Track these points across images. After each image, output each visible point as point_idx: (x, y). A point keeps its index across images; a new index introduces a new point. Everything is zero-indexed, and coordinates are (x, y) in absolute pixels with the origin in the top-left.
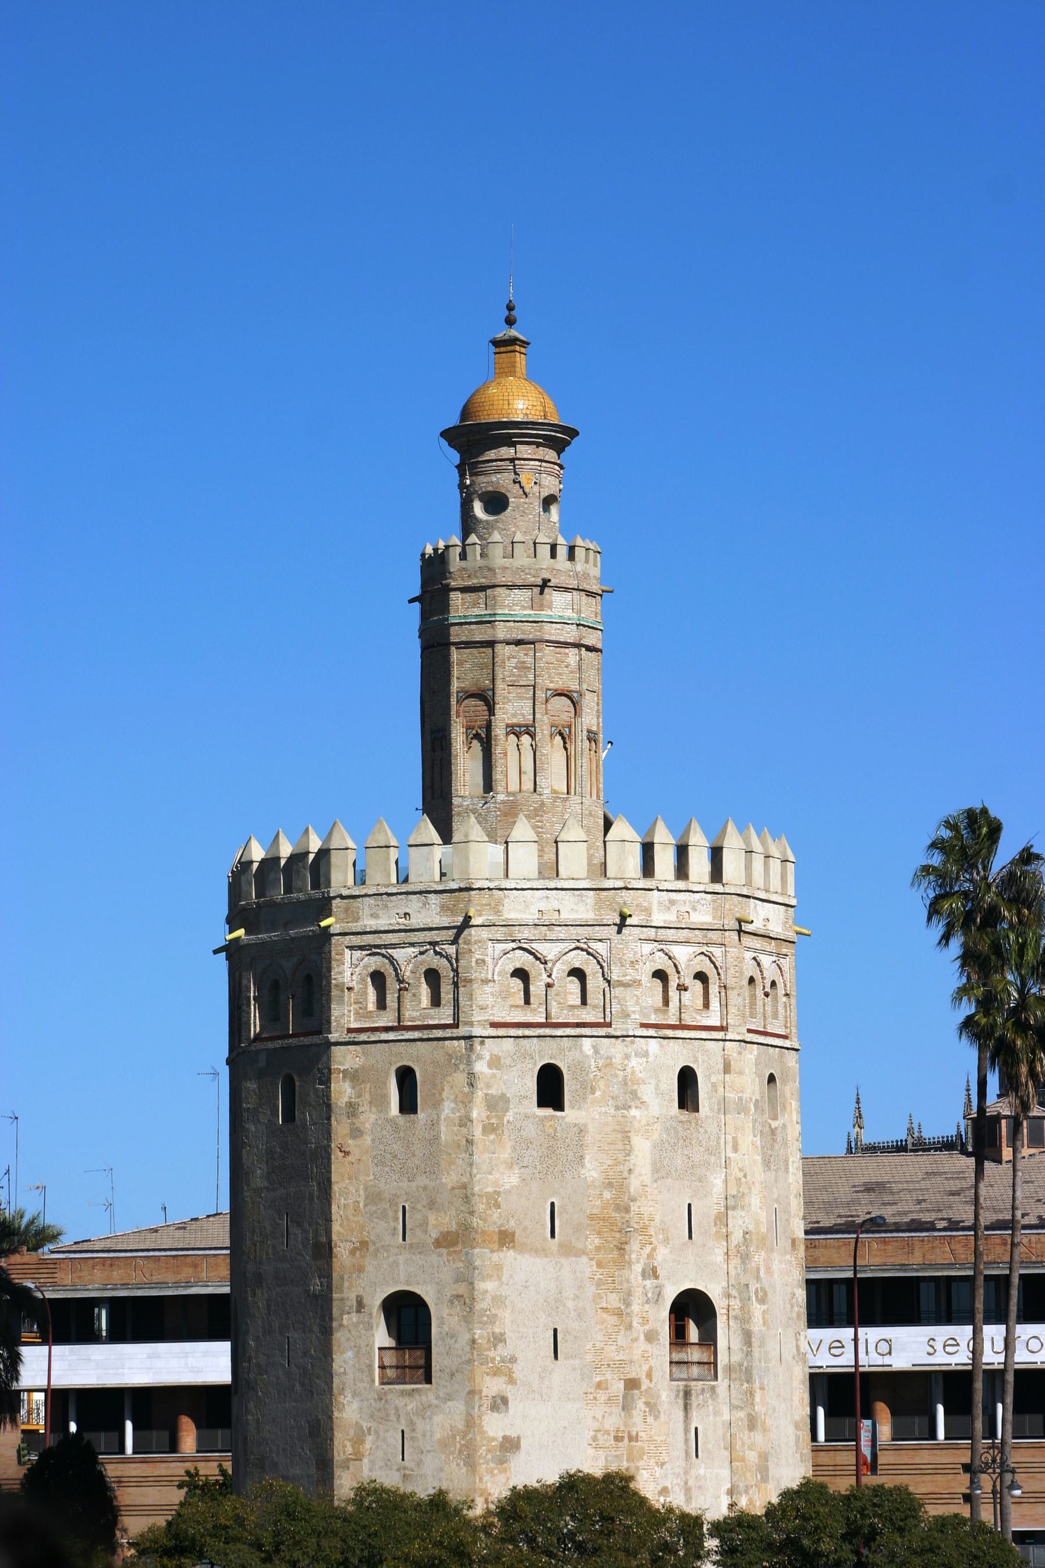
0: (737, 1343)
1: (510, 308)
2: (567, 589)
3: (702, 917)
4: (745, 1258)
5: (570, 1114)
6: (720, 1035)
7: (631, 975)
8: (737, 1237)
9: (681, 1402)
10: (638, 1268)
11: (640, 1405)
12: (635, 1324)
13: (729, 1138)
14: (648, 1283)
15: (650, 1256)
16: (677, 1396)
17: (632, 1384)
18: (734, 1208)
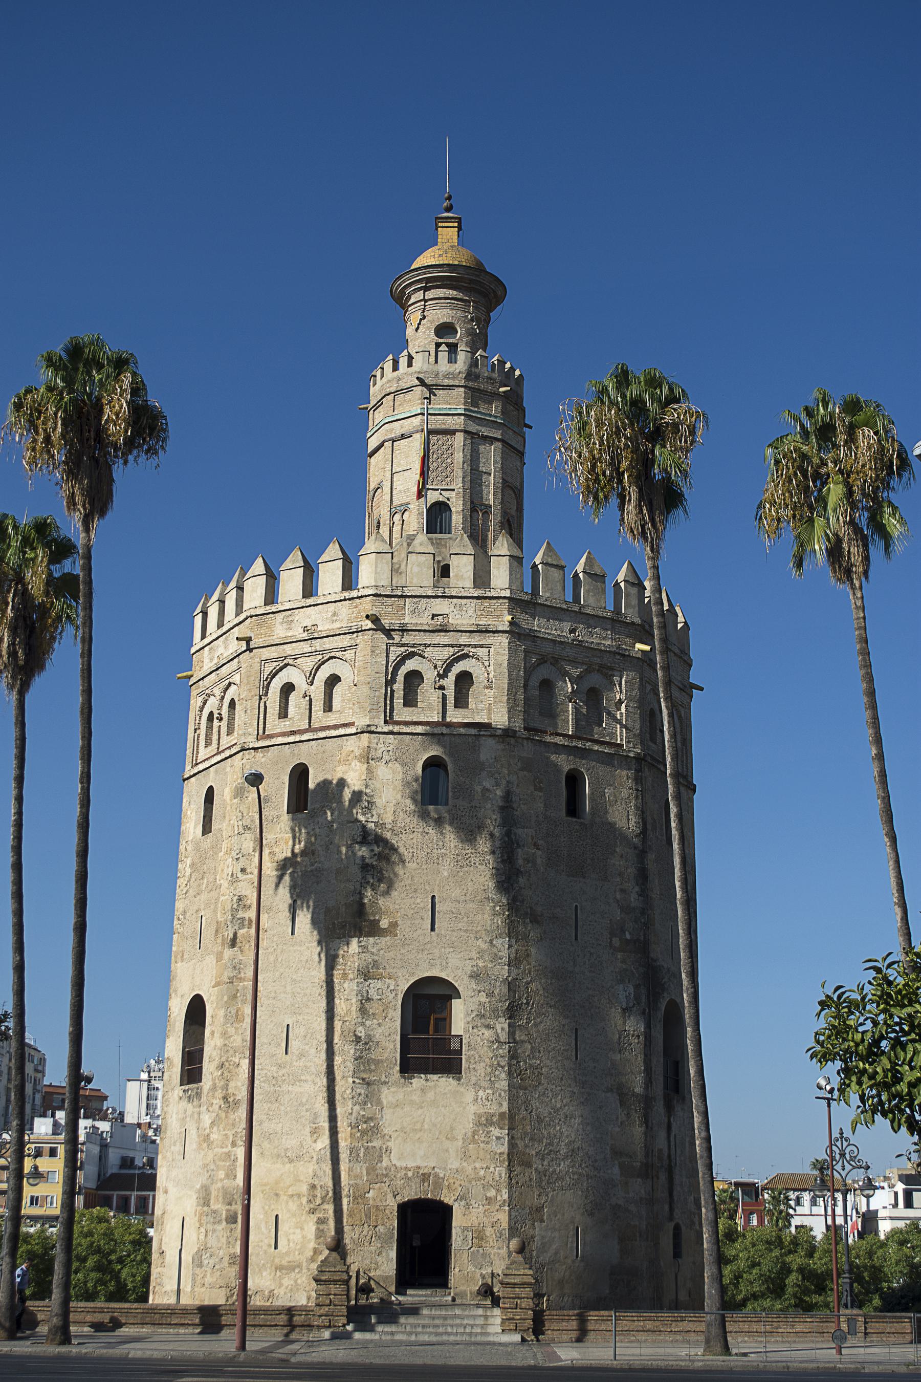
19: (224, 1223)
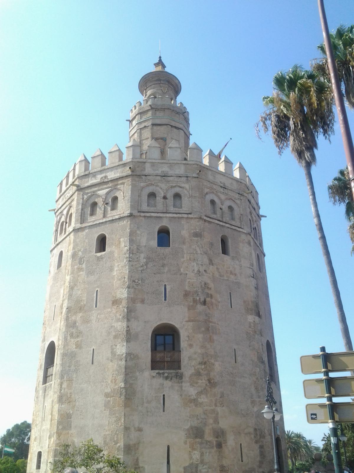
19: (215, 448)
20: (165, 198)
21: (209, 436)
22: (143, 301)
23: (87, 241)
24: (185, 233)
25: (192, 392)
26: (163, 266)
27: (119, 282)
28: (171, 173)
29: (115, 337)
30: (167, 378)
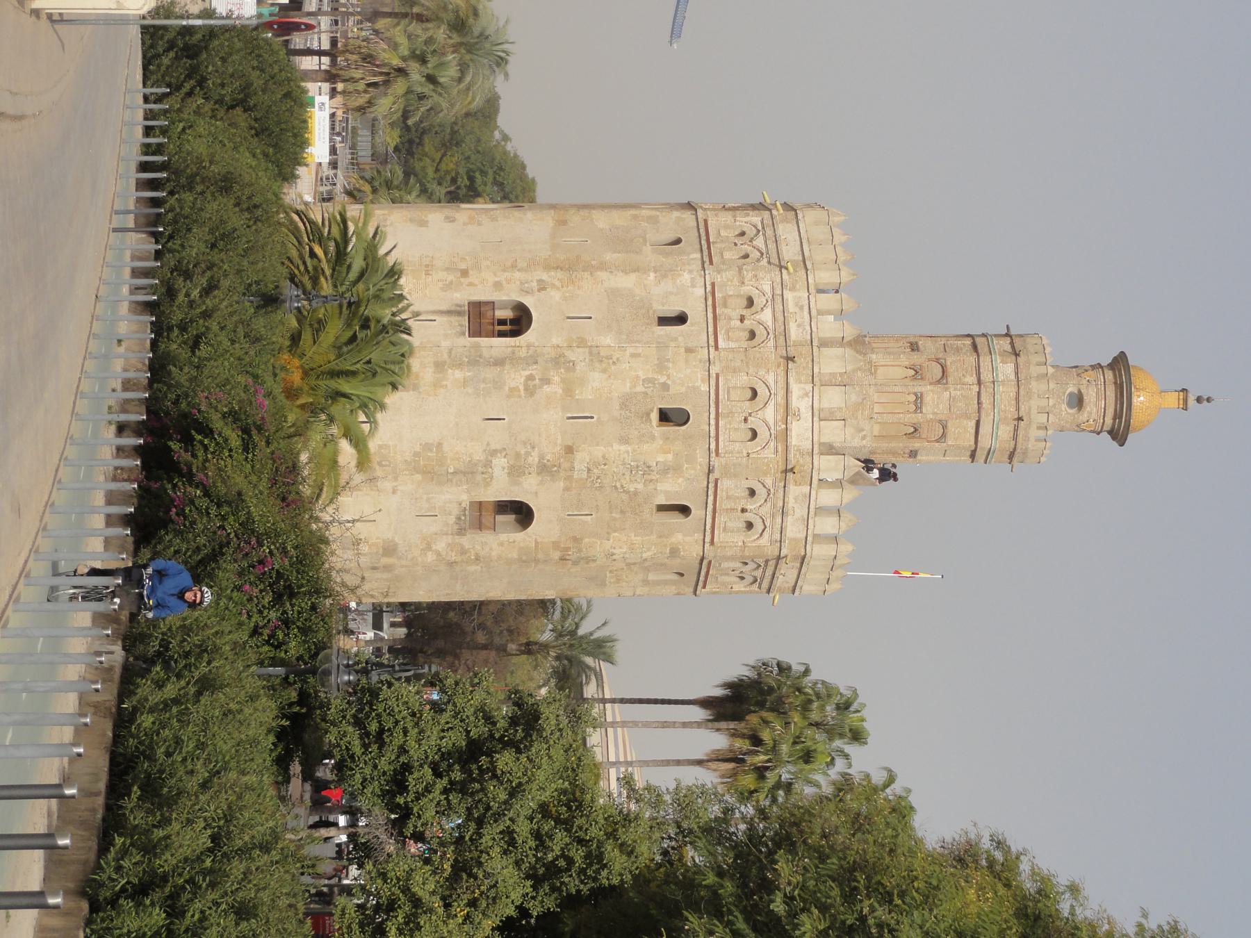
0: (496, 353)
1: (1209, 400)
2: (1017, 373)
3: (794, 333)
4: (558, 361)
5: (648, 249)
6: (712, 343)
7: (748, 275)
8: (571, 355)
9: (453, 308)
10: (545, 277)
11: (450, 278)
12: (506, 274)
13: (640, 350)
14: (535, 284)
15: (553, 286)
16: (457, 305)
17: (465, 273)
18: (591, 353)
20: (743, 510)
21: (385, 561)
22: (567, 489)
23: (683, 390)
24: (678, 537)
25: (440, 546)
26: (622, 512)
27: (600, 455)
28: (789, 520)
29: (518, 455)
30: (459, 519)
